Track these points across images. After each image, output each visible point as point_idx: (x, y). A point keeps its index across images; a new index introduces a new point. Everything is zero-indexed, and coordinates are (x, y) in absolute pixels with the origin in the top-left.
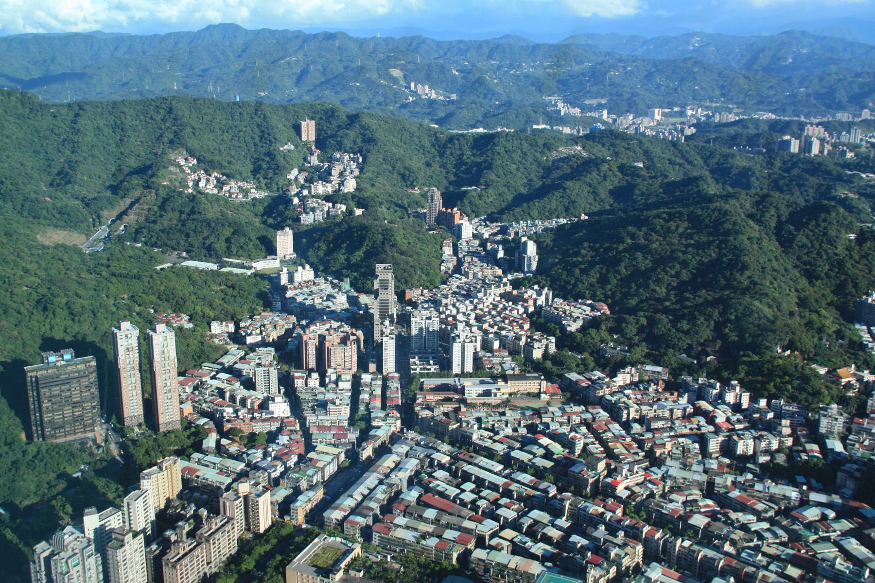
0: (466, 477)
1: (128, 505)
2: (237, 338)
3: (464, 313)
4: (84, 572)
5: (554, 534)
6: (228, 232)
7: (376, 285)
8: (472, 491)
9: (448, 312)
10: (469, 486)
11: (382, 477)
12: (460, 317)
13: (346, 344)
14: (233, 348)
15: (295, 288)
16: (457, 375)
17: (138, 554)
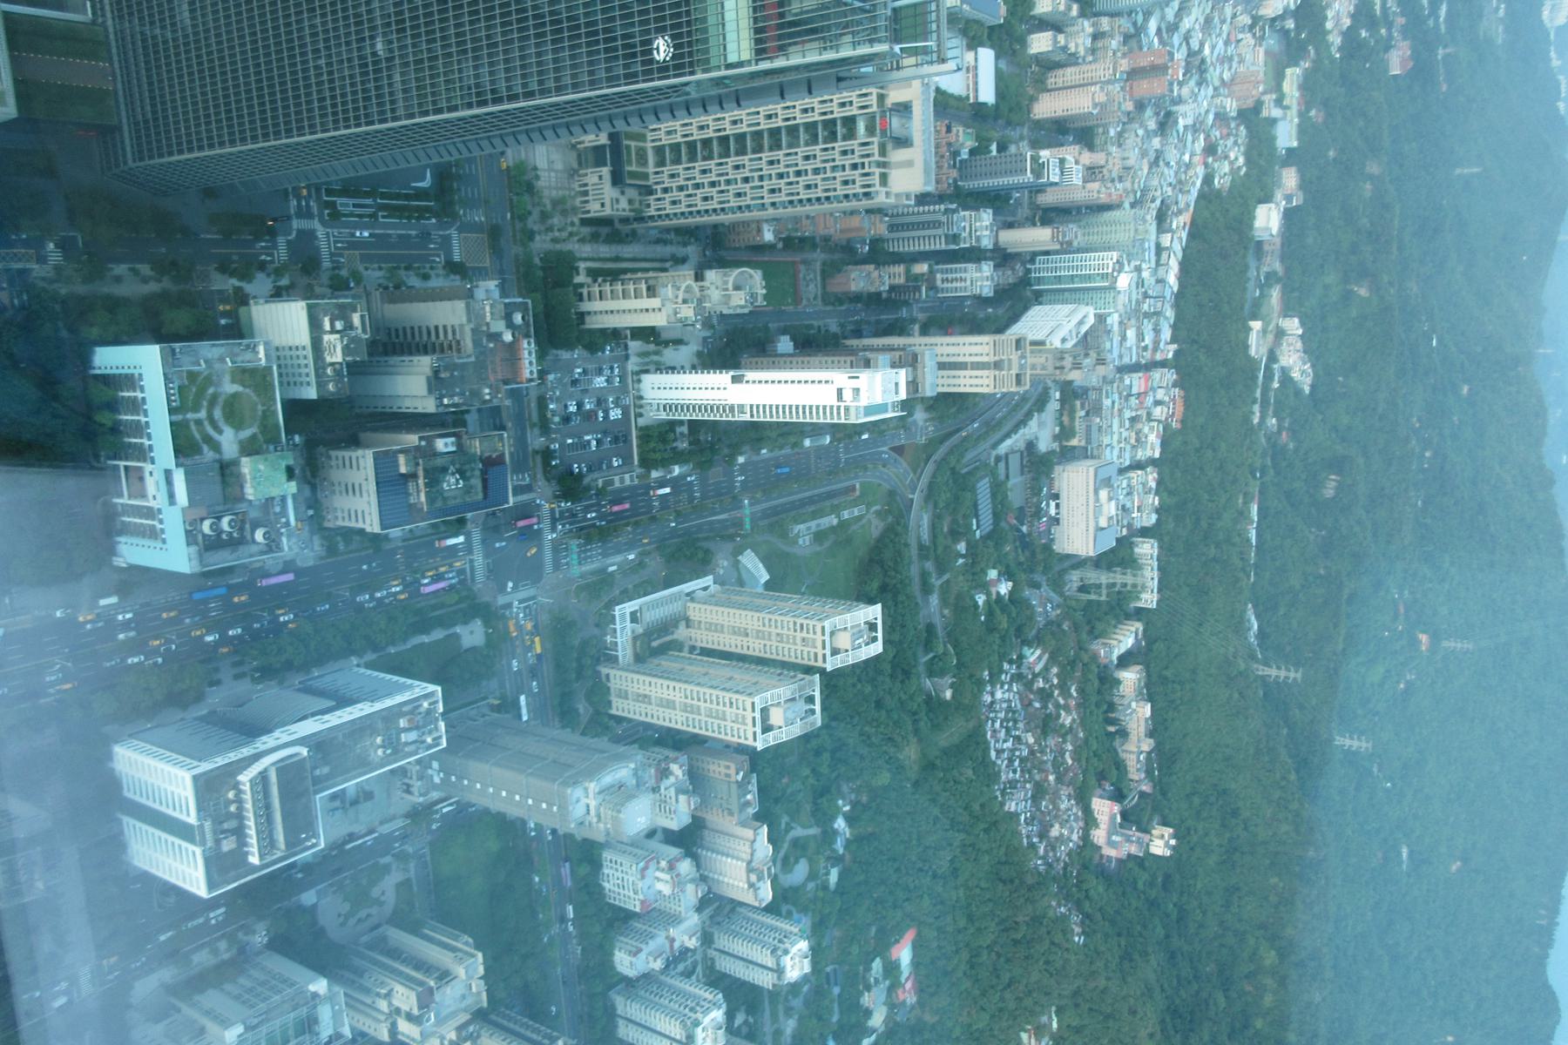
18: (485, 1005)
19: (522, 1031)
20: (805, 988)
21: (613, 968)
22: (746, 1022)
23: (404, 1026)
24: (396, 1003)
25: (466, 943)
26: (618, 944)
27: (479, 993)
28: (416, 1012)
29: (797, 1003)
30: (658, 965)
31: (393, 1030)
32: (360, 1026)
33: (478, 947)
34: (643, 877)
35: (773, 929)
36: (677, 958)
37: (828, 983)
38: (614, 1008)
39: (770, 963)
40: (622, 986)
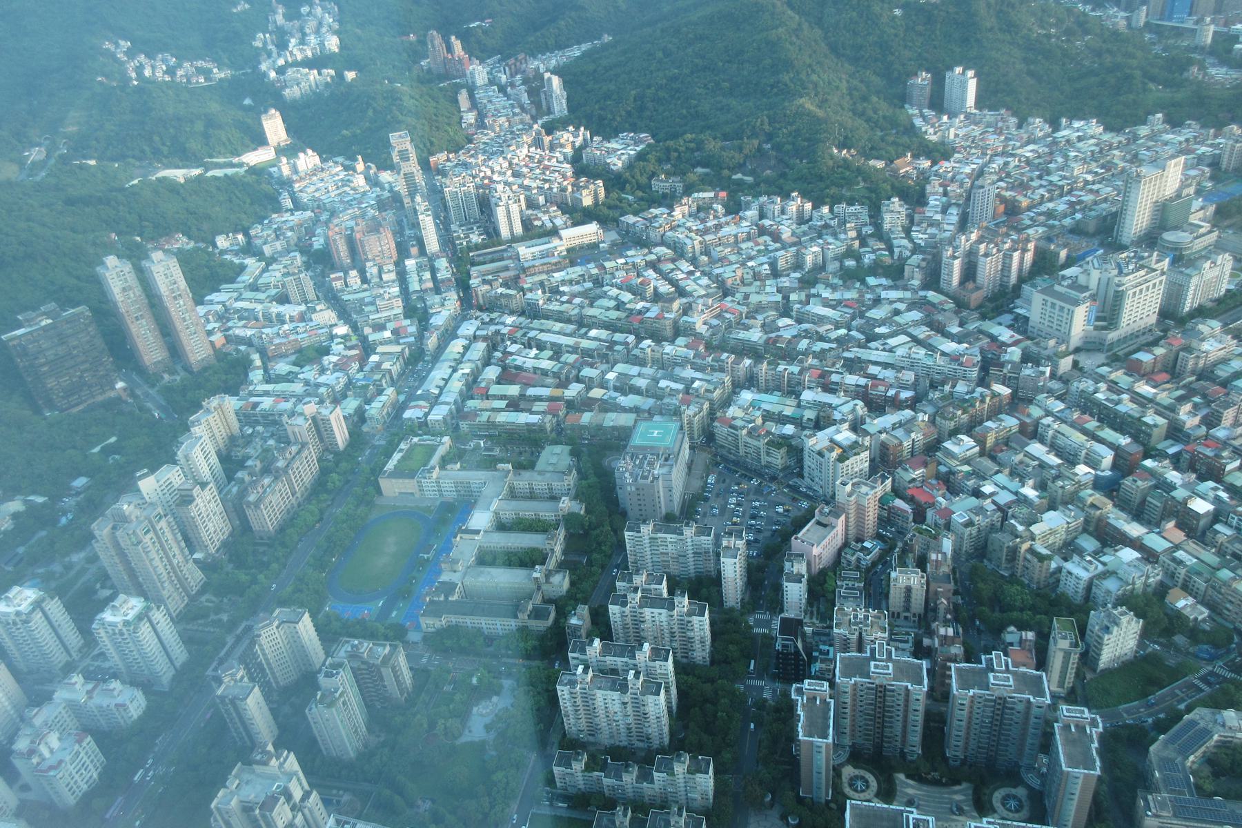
0: (541, 346)
1: (187, 458)
2: (249, 249)
3: (500, 173)
4: (158, 538)
5: (642, 383)
6: (199, 126)
7: (396, 158)
8: (550, 359)
9: (482, 174)
10: (548, 353)
11: (453, 364)
12: (495, 177)
13: (378, 232)
14: (250, 262)
15: (301, 179)
16: (508, 242)
17: (212, 505)
18: (239, 764)
19: (237, 720)
20: (40, 571)
21: (148, 707)
22: (103, 587)
23: (297, 794)
24: (290, 815)
25: (216, 820)
26: (129, 722)
27: (236, 777)
28: (282, 799)
29: (57, 568)
30: (115, 685)
31: (306, 796)
32: (325, 814)
33: (211, 813)
34: (61, 762)
35: (12, 637)
36: (97, 676)
37: (21, 560)
38: (174, 678)
39: (38, 616)
40: (155, 688)
